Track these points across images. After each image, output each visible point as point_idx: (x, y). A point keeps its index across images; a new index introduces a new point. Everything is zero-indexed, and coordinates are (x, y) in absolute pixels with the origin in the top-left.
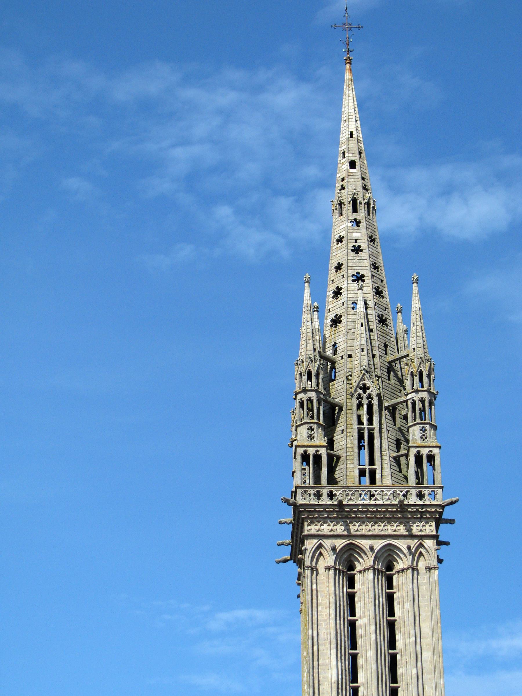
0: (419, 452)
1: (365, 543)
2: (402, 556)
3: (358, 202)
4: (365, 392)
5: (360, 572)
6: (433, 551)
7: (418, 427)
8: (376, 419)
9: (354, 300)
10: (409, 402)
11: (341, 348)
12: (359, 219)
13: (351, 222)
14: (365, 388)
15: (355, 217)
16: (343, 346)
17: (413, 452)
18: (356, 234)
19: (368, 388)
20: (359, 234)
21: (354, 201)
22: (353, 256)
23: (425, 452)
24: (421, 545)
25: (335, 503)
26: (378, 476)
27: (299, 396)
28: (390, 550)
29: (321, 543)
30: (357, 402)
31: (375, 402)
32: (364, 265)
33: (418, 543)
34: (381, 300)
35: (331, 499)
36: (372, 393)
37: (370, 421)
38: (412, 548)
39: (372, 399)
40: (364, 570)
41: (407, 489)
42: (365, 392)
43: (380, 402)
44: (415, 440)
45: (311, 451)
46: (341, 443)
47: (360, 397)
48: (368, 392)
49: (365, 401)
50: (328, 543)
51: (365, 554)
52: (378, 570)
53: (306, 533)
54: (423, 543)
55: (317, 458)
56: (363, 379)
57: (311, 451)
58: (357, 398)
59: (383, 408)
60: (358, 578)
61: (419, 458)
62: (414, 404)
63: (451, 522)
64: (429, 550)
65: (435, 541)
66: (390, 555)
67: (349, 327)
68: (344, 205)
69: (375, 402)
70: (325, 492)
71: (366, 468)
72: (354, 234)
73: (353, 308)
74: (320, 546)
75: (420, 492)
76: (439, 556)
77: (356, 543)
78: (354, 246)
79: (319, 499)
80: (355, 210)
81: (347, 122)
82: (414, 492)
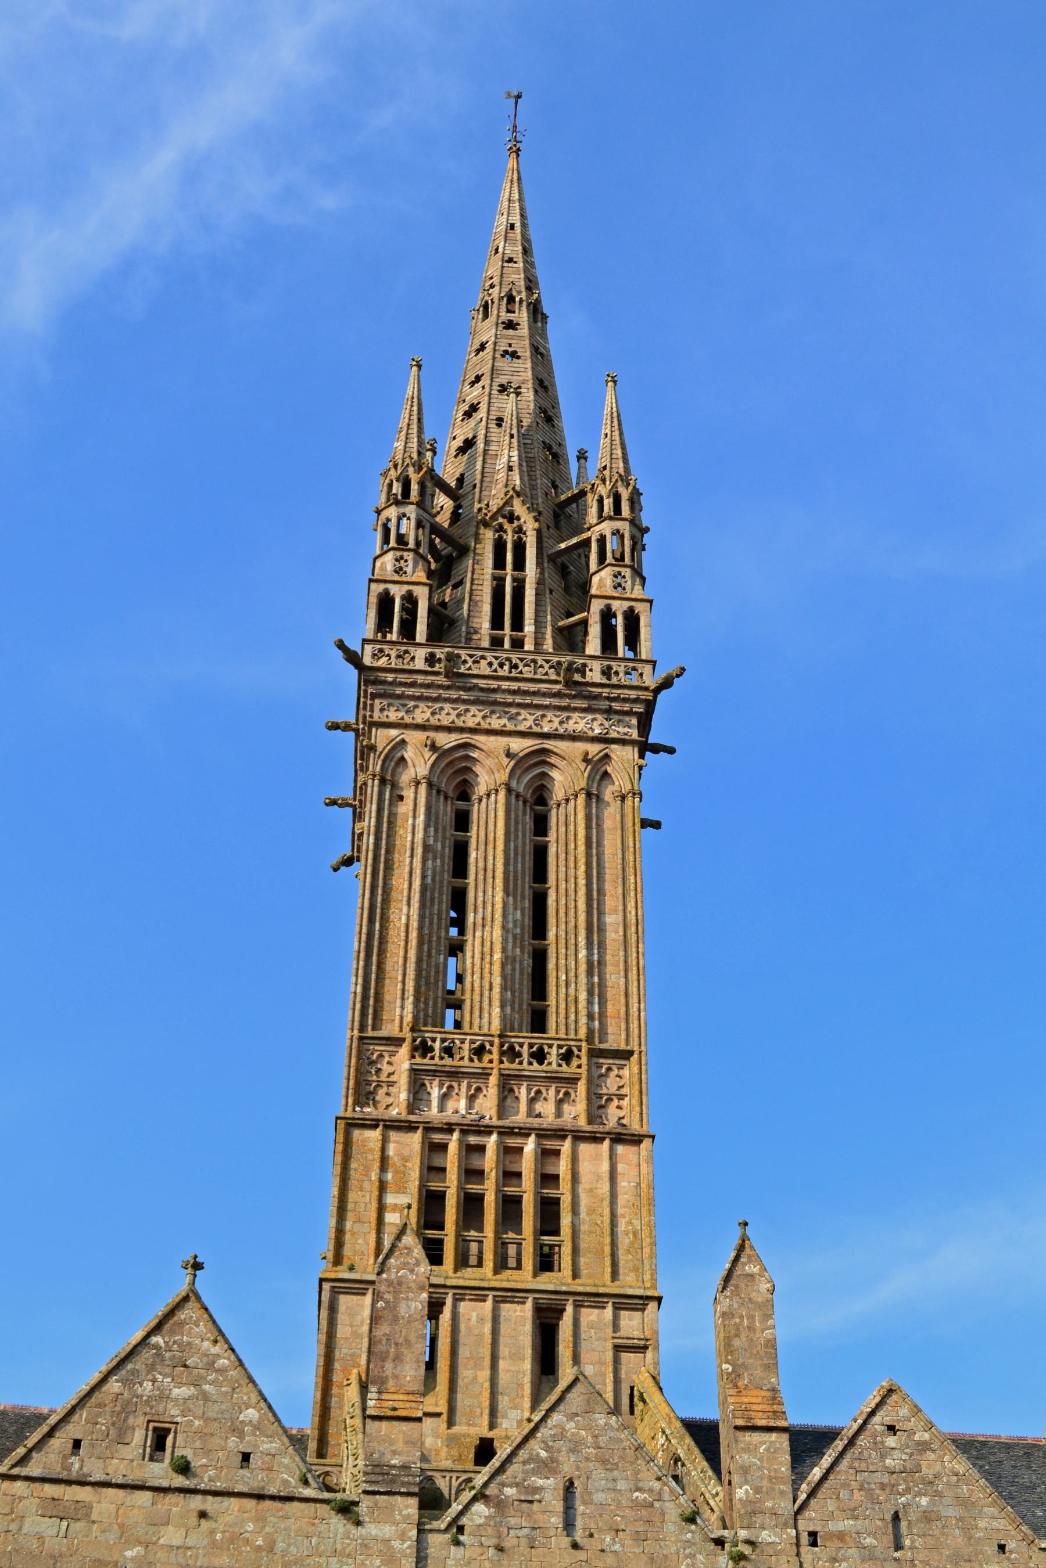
9: (499, 414)
14: (511, 518)
17: (596, 607)
23: (619, 607)
27: (385, 514)
30: (496, 536)
35: (432, 665)
44: (600, 586)
45: (397, 592)
47: (501, 529)
48: (516, 523)
49: (509, 538)
52: (518, 796)
55: (410, 601)
56: (508, 502)
61: (607, 615)
65: (636, 749)
70: (421, 654)
71: (505, 635)
78: (506, 352)
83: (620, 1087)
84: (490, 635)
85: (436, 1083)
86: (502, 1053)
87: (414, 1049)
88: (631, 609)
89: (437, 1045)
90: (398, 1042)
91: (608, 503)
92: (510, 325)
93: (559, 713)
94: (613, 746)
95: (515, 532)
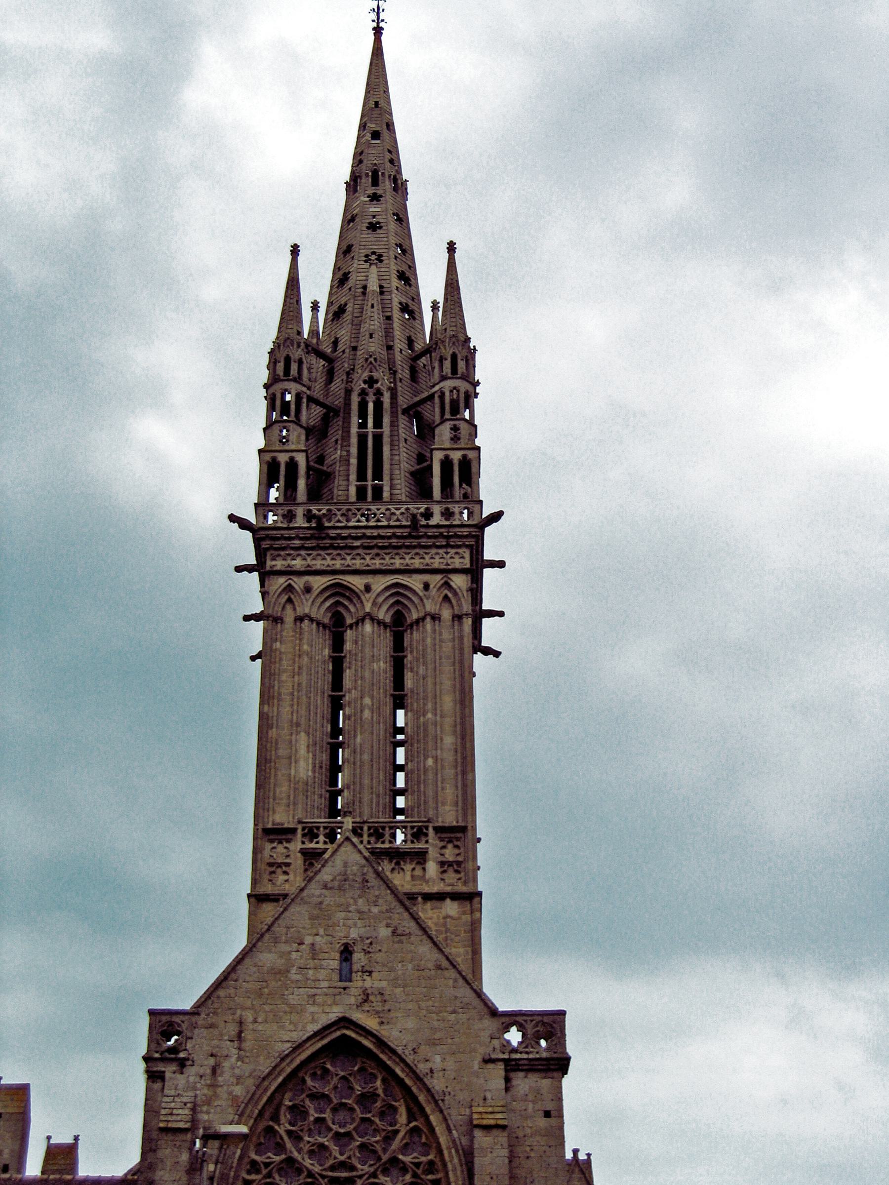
0: (447, 457)
1: (357, 582)
2: (414, 599)
3: (380, 173)
4: (371, 387)
5: (351, 626)
6: (465, 593)
7: (448, 425)
8: (386, 420)
10: (436, 396)
11: (343, 340)
12: (379, 192)
13: (368, 197)
14: (371, 381)
16: (346, 338)
17: (438, 456)
18: (374, 209)
19: (377, 381)
20: (378, 210)
21: (375, 174)
22: (368, 236)
23: (456, 456)
24: (447, 585)
25: (314, 525)
26: (386, 495)
29: (290, 585)
31: (386, 399)
32: (383, 243)
33: (442, 582)
34: (408, 287)
35: (309, 521)
36: (382, 387)
37: (378, 423)
38: (431, 586)
39: (382, 394)
40: (357, 623)
41: (426, 506)
42: (371, 387)
43: (394, 397)
45: (283, 458)
46: (333, 457)
50: (299, 583)
51: (359, 598)
53: (268, 568)
54: (449, 581)
55: (292, 465)
57: (283, 458)
58: (359, 395)
59: (399, 409)
60: (349, 635)
61: (446, 464)
62: (442, 395)
63: (501, 564)
64: (458, 590)
67: (356, 315)
68: (361, 179)
69: (386, 399)
72: (371, 210)
73: (364, 294)
74: (289, 588)
75: (447, 509)
76: (497, 657)
77: (345, 583)
78: (370, 223)
79: (290, 521)
80: (375, 183)
81: (371, 92)
82: (437, 509)
83: (458, 855)
84: (356, 486)
86: (370, 835)
87: (304, 835)
88: (464, 456)
91: (447, 364)
92: (375, 198)
93: (408, 551)
94: (451, 576)
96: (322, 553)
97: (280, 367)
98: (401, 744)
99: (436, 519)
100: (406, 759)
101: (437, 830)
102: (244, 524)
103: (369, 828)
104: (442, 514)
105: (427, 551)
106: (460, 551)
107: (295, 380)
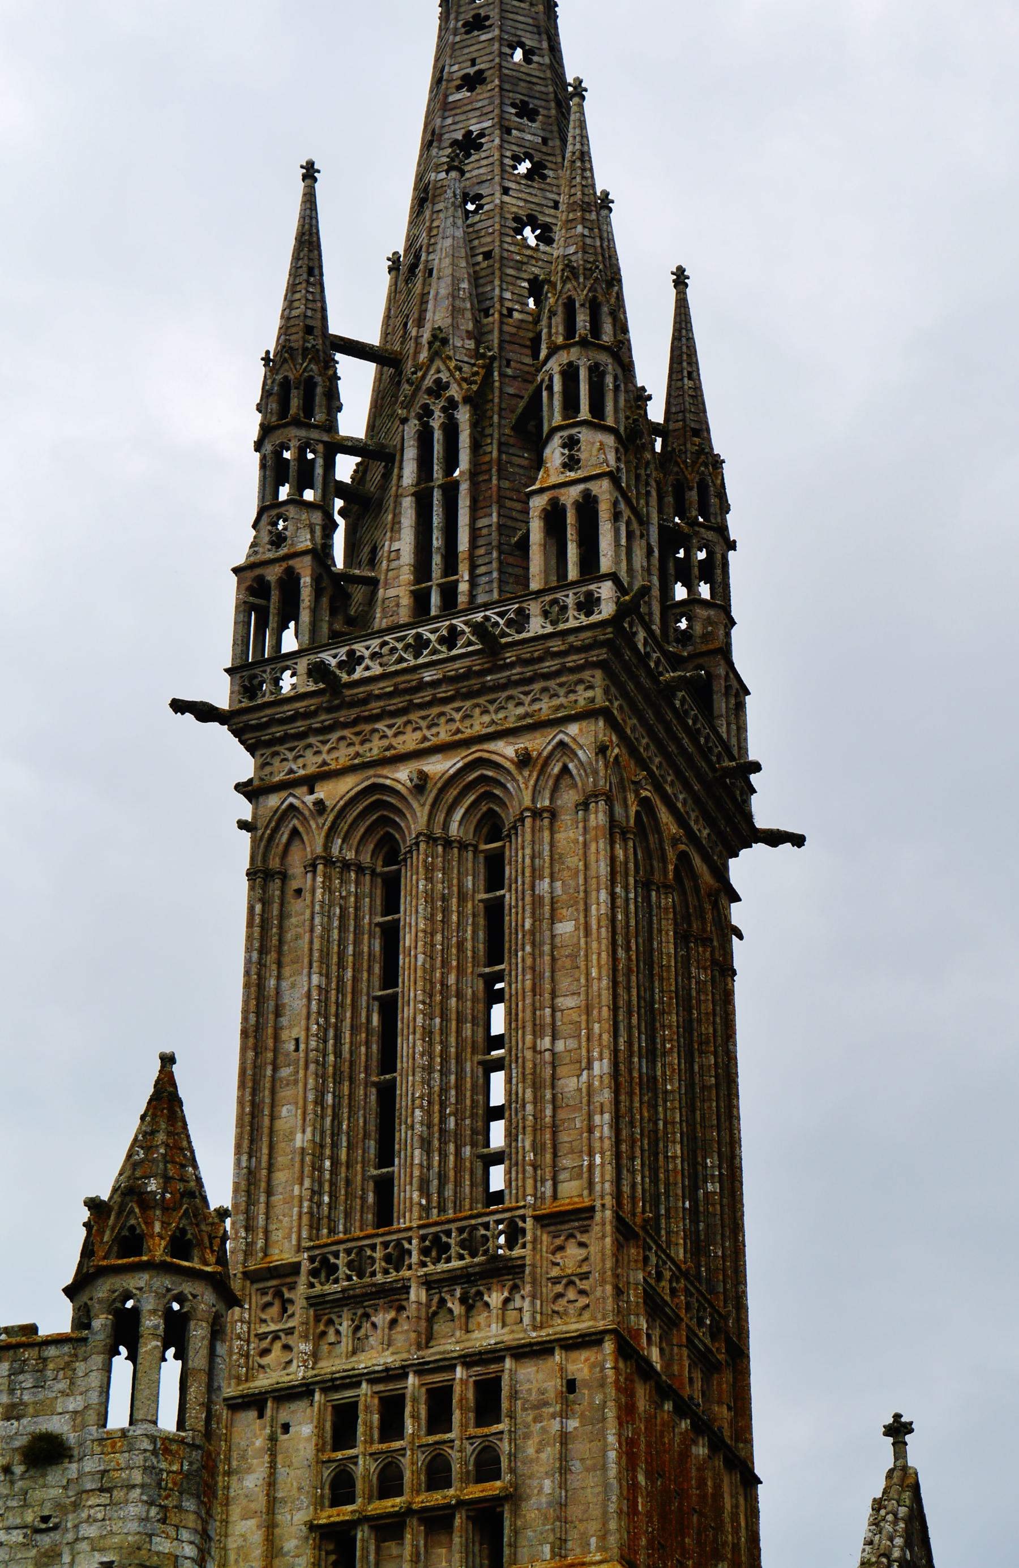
0: (554, 503)
15: (473, 13)
17: (538, 503)
26: (462, 599)
28: (483, 778)
49: (436, 422)
57: (273, 574)
66: (488, 796)
85: (346, 1314)
89: (341, 1261)
90: (294, 1269)
95: (444, 409)
96: (346, 733)
97: (274, 406)
98: (498, 1065)
99: (537, 626)
100: (509, 1093)
101: (543, 1220)
102: (204, 712)
103: (423, 1238)
104: (545, 614)
105: (526, 689)
106: (586, 675)
107: (297, 423)
